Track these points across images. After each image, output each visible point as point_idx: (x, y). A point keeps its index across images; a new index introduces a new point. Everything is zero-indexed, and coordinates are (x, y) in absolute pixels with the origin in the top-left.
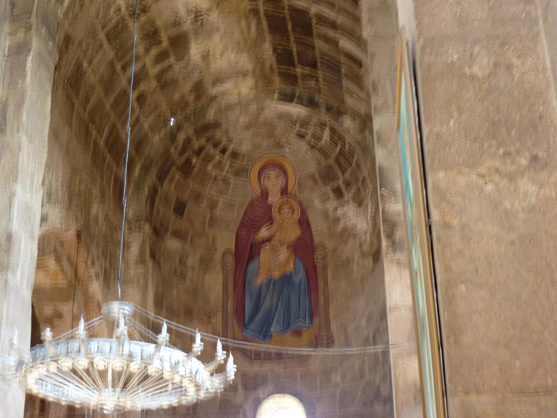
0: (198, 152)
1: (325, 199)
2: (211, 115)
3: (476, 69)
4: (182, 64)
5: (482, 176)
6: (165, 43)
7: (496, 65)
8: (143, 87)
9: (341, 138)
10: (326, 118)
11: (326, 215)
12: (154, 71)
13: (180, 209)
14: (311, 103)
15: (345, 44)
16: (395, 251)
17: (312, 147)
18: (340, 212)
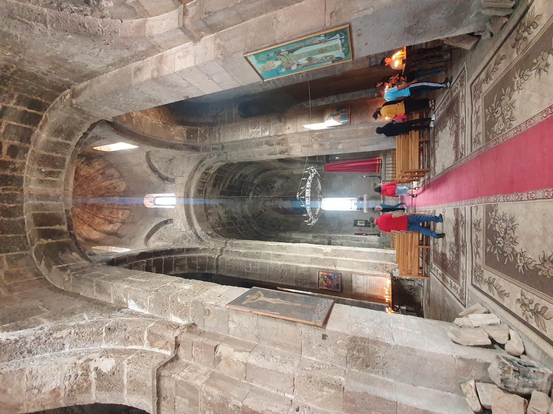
0: (260, 220)
1: (273, 191)
2: (250, 215)
3: (253, 35)
4: (238, 219)
5: (277, 29)
6: (232, 221)
7: (252, 31)
8: (243, 229)
9: (259, 184)
10: (254, 187)
11: (277, 192)
12: (239, 225)
13: (273, 226)
14: (250, 191)
15: (237, 177)
17: (260, 193)
18: (276, 188)
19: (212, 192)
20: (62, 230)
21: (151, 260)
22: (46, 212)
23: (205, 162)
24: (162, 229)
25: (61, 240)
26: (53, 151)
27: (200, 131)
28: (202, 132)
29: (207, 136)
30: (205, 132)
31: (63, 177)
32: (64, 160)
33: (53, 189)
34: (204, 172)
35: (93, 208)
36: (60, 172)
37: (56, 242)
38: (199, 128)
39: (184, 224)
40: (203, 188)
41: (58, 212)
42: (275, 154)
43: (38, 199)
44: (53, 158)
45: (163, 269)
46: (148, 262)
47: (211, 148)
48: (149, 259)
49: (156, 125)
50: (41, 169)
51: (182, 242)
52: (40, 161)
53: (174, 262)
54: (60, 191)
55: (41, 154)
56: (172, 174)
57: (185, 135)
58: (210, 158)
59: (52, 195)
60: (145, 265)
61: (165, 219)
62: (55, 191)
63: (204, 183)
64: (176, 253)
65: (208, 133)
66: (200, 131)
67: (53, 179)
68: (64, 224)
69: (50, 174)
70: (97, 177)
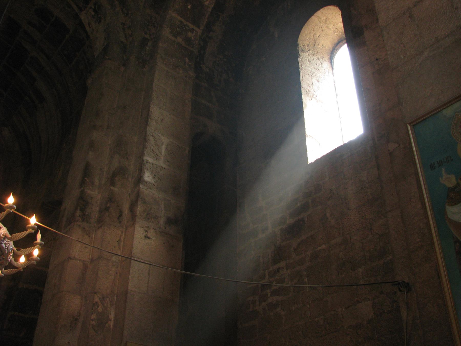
16: (83, 221)
28: (190, 34)
29: (179, 40)
30: (188, 41)
38: (199, 32)
42: (83, 183)
47: (147, 36)
65: (183, 44)
66: (192, 31)
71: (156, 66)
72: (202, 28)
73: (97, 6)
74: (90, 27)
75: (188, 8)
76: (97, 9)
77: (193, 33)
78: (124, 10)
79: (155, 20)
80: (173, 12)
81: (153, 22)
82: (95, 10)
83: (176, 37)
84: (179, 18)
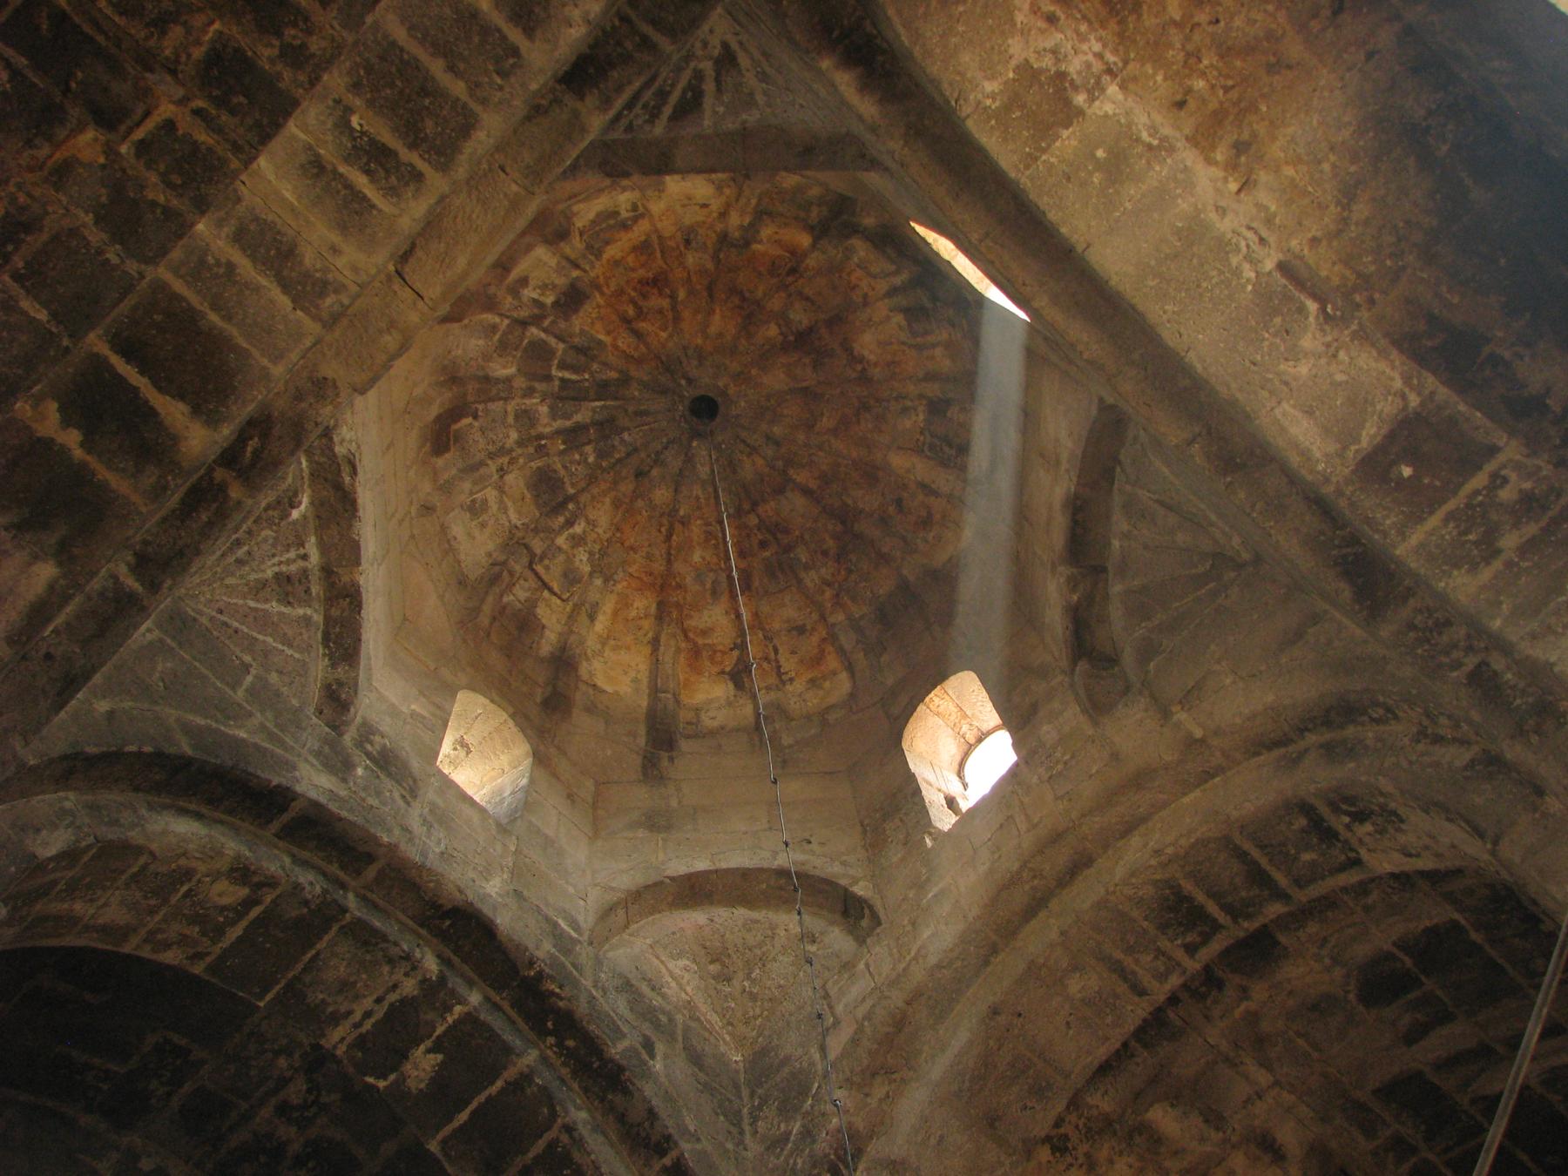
19: (1320, 1007)
20: (175, 440)
21: (462, 1001)
22: (214, 317)
23: (1369, 734)
24: (787, 922)
25: (104, 474)
26: (442, 50)
27: (1498, 480)
28: (1506, 494)
29: (1509, 541)
31: (412, 212)
32: (467, 127)
33: (335, 237)
34: (1306, 809)
35: (763, 545)
36: (418, 177)
37: (83, 465)
38: (1511, 450)
39: (868, 1016)
40: (1235, 912)
41: (255, 353)
43: (239, 237)
44: (428, 88)
45: (463, 1116)
46: (434, 992)
47: (1471, 662)
48: (455, 982)
49: (1223, 247)
50: (349, 110)
51: (764, 1101)
52: (369, 69)
53: (540, 1145)
54: (355, 269)
55: (386, 37)
56: (1147, 651)
57: (1370, 434)
58: (1422, 734)
59: (307, 262)
60: (409, 987)
61: (860, 890)
62: (335, 250)
63: (1258, 877)
64: (621, 1118)
65: (1532, 529)
66: (1498, 480)
67: (370, 191)
68: (212, 421)
69: (375, 156)
70: (905, 410)
71: (1556, 669)
72: (1501, 438)
73: (1344, 807)
74: (1418, 855)
75: (1410, 477)
76: (1353, 809)
77: (1505, 480)
78: (1375, 715)
79: (1426, 615)
80: (1404, 540)
81: (1430, 623)
82: (1360, 817)
83: (1498, 552)
84: (1434, 521)
